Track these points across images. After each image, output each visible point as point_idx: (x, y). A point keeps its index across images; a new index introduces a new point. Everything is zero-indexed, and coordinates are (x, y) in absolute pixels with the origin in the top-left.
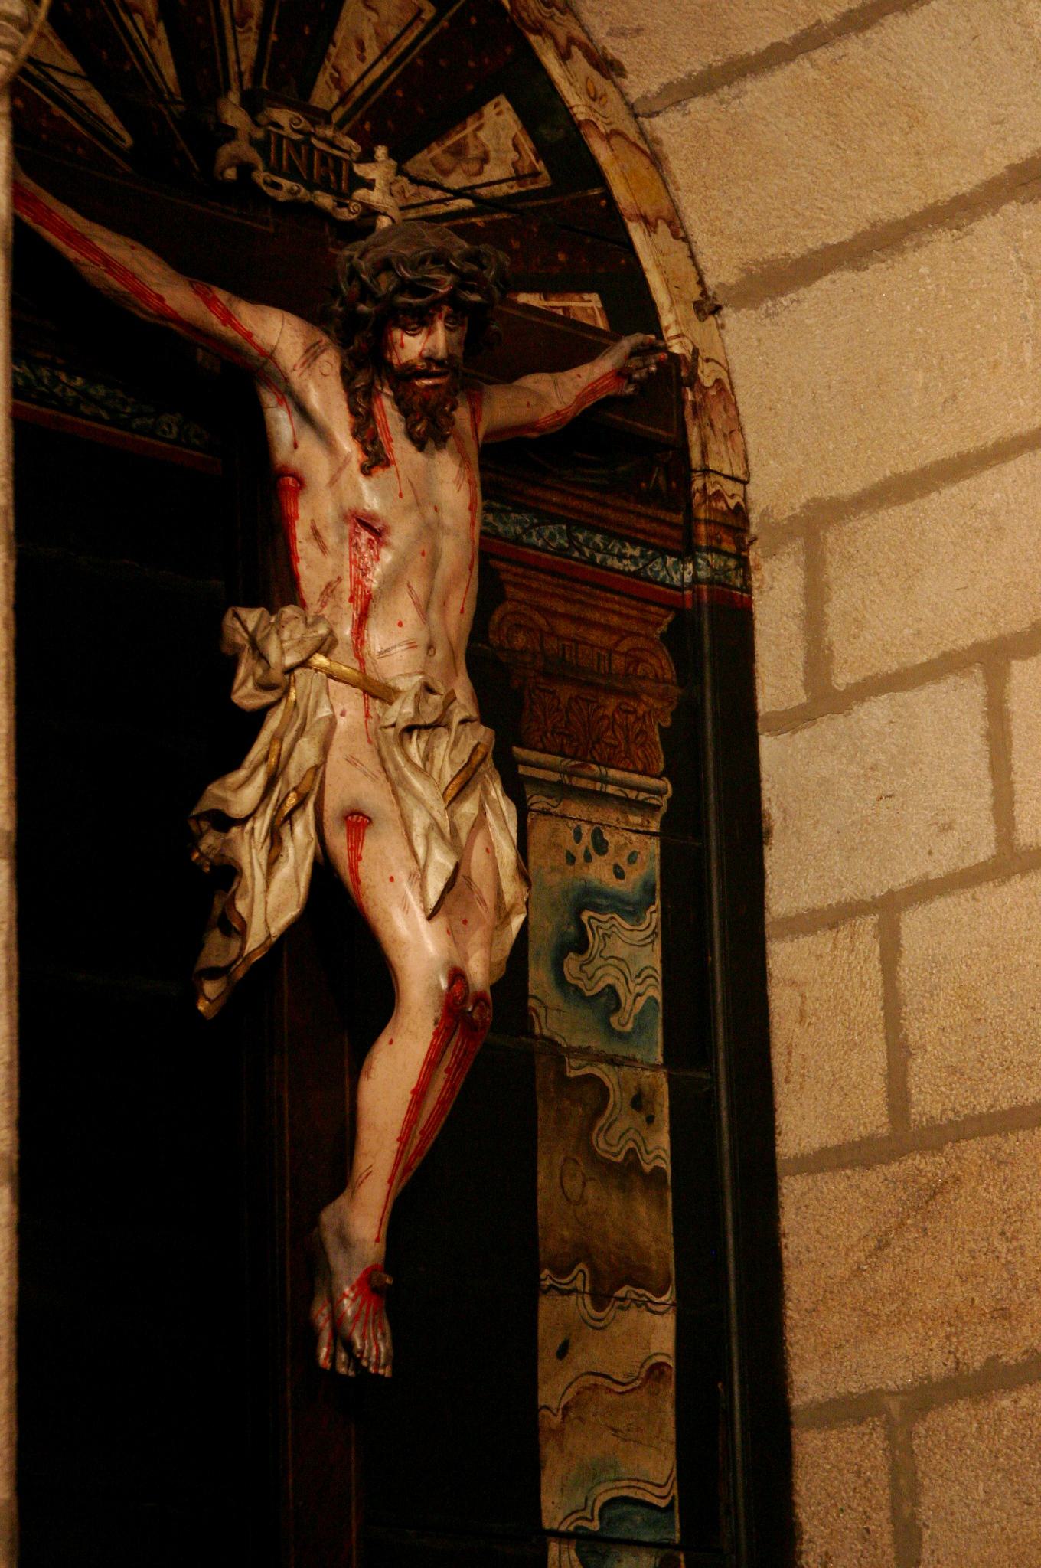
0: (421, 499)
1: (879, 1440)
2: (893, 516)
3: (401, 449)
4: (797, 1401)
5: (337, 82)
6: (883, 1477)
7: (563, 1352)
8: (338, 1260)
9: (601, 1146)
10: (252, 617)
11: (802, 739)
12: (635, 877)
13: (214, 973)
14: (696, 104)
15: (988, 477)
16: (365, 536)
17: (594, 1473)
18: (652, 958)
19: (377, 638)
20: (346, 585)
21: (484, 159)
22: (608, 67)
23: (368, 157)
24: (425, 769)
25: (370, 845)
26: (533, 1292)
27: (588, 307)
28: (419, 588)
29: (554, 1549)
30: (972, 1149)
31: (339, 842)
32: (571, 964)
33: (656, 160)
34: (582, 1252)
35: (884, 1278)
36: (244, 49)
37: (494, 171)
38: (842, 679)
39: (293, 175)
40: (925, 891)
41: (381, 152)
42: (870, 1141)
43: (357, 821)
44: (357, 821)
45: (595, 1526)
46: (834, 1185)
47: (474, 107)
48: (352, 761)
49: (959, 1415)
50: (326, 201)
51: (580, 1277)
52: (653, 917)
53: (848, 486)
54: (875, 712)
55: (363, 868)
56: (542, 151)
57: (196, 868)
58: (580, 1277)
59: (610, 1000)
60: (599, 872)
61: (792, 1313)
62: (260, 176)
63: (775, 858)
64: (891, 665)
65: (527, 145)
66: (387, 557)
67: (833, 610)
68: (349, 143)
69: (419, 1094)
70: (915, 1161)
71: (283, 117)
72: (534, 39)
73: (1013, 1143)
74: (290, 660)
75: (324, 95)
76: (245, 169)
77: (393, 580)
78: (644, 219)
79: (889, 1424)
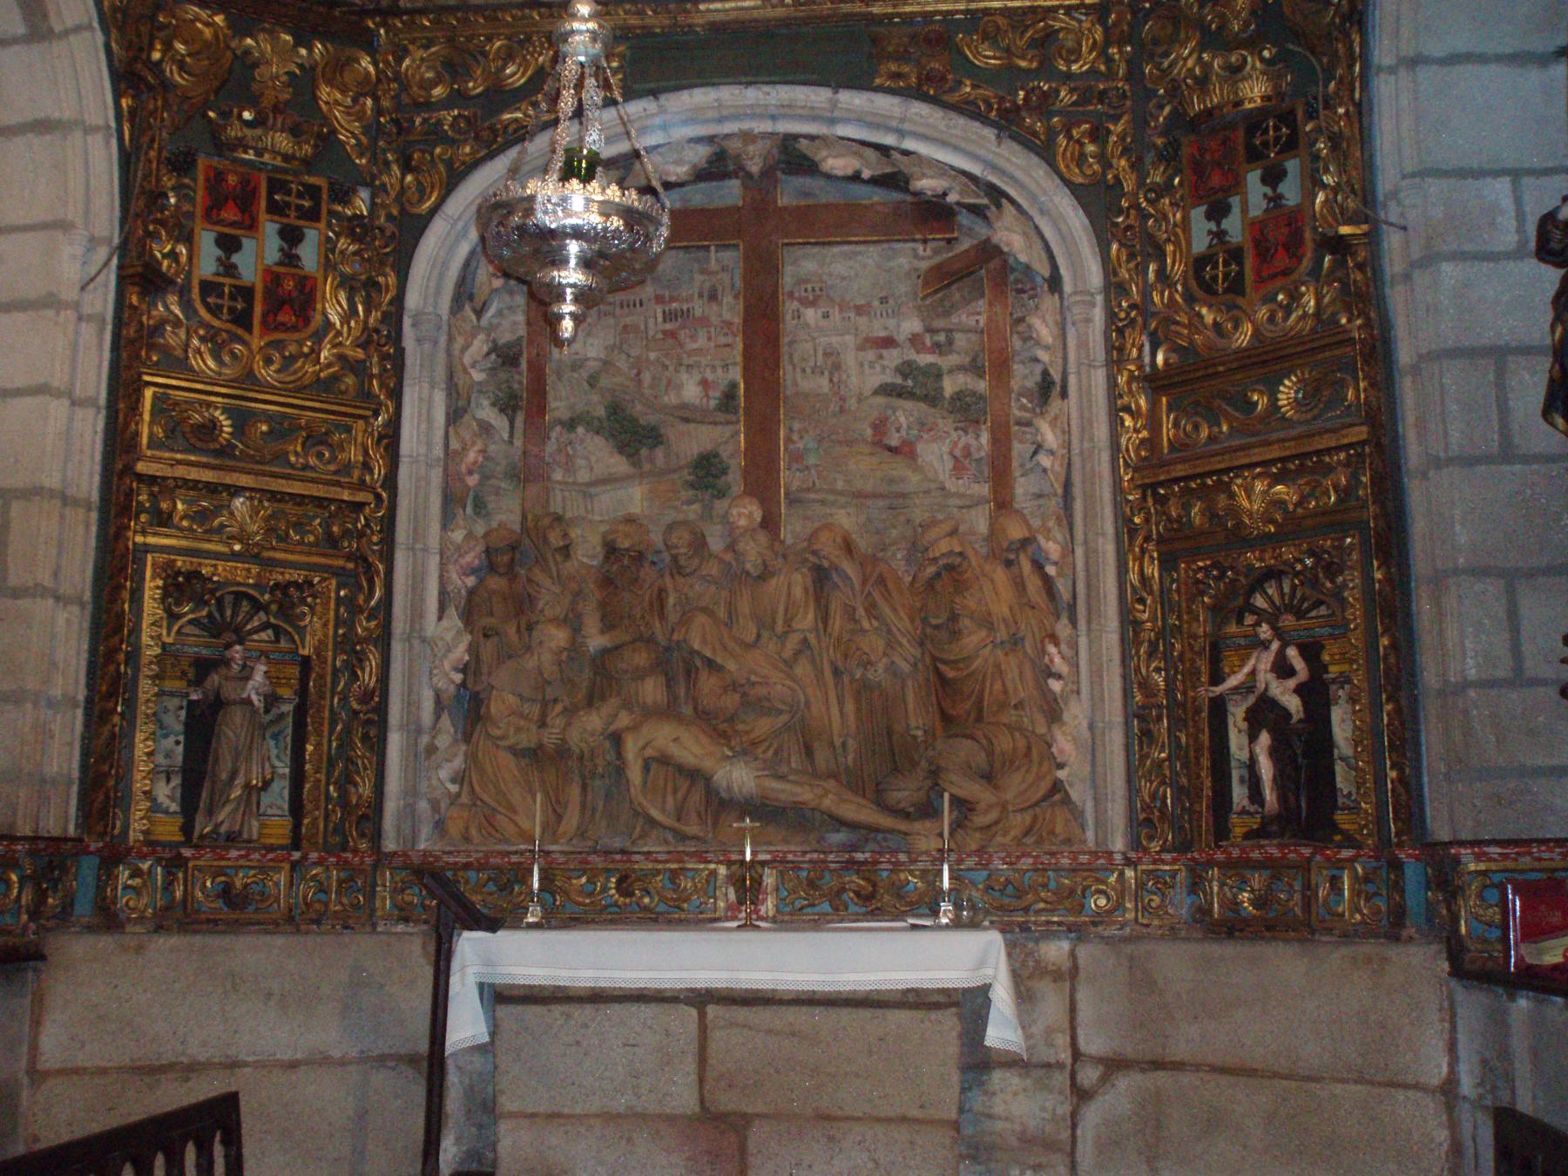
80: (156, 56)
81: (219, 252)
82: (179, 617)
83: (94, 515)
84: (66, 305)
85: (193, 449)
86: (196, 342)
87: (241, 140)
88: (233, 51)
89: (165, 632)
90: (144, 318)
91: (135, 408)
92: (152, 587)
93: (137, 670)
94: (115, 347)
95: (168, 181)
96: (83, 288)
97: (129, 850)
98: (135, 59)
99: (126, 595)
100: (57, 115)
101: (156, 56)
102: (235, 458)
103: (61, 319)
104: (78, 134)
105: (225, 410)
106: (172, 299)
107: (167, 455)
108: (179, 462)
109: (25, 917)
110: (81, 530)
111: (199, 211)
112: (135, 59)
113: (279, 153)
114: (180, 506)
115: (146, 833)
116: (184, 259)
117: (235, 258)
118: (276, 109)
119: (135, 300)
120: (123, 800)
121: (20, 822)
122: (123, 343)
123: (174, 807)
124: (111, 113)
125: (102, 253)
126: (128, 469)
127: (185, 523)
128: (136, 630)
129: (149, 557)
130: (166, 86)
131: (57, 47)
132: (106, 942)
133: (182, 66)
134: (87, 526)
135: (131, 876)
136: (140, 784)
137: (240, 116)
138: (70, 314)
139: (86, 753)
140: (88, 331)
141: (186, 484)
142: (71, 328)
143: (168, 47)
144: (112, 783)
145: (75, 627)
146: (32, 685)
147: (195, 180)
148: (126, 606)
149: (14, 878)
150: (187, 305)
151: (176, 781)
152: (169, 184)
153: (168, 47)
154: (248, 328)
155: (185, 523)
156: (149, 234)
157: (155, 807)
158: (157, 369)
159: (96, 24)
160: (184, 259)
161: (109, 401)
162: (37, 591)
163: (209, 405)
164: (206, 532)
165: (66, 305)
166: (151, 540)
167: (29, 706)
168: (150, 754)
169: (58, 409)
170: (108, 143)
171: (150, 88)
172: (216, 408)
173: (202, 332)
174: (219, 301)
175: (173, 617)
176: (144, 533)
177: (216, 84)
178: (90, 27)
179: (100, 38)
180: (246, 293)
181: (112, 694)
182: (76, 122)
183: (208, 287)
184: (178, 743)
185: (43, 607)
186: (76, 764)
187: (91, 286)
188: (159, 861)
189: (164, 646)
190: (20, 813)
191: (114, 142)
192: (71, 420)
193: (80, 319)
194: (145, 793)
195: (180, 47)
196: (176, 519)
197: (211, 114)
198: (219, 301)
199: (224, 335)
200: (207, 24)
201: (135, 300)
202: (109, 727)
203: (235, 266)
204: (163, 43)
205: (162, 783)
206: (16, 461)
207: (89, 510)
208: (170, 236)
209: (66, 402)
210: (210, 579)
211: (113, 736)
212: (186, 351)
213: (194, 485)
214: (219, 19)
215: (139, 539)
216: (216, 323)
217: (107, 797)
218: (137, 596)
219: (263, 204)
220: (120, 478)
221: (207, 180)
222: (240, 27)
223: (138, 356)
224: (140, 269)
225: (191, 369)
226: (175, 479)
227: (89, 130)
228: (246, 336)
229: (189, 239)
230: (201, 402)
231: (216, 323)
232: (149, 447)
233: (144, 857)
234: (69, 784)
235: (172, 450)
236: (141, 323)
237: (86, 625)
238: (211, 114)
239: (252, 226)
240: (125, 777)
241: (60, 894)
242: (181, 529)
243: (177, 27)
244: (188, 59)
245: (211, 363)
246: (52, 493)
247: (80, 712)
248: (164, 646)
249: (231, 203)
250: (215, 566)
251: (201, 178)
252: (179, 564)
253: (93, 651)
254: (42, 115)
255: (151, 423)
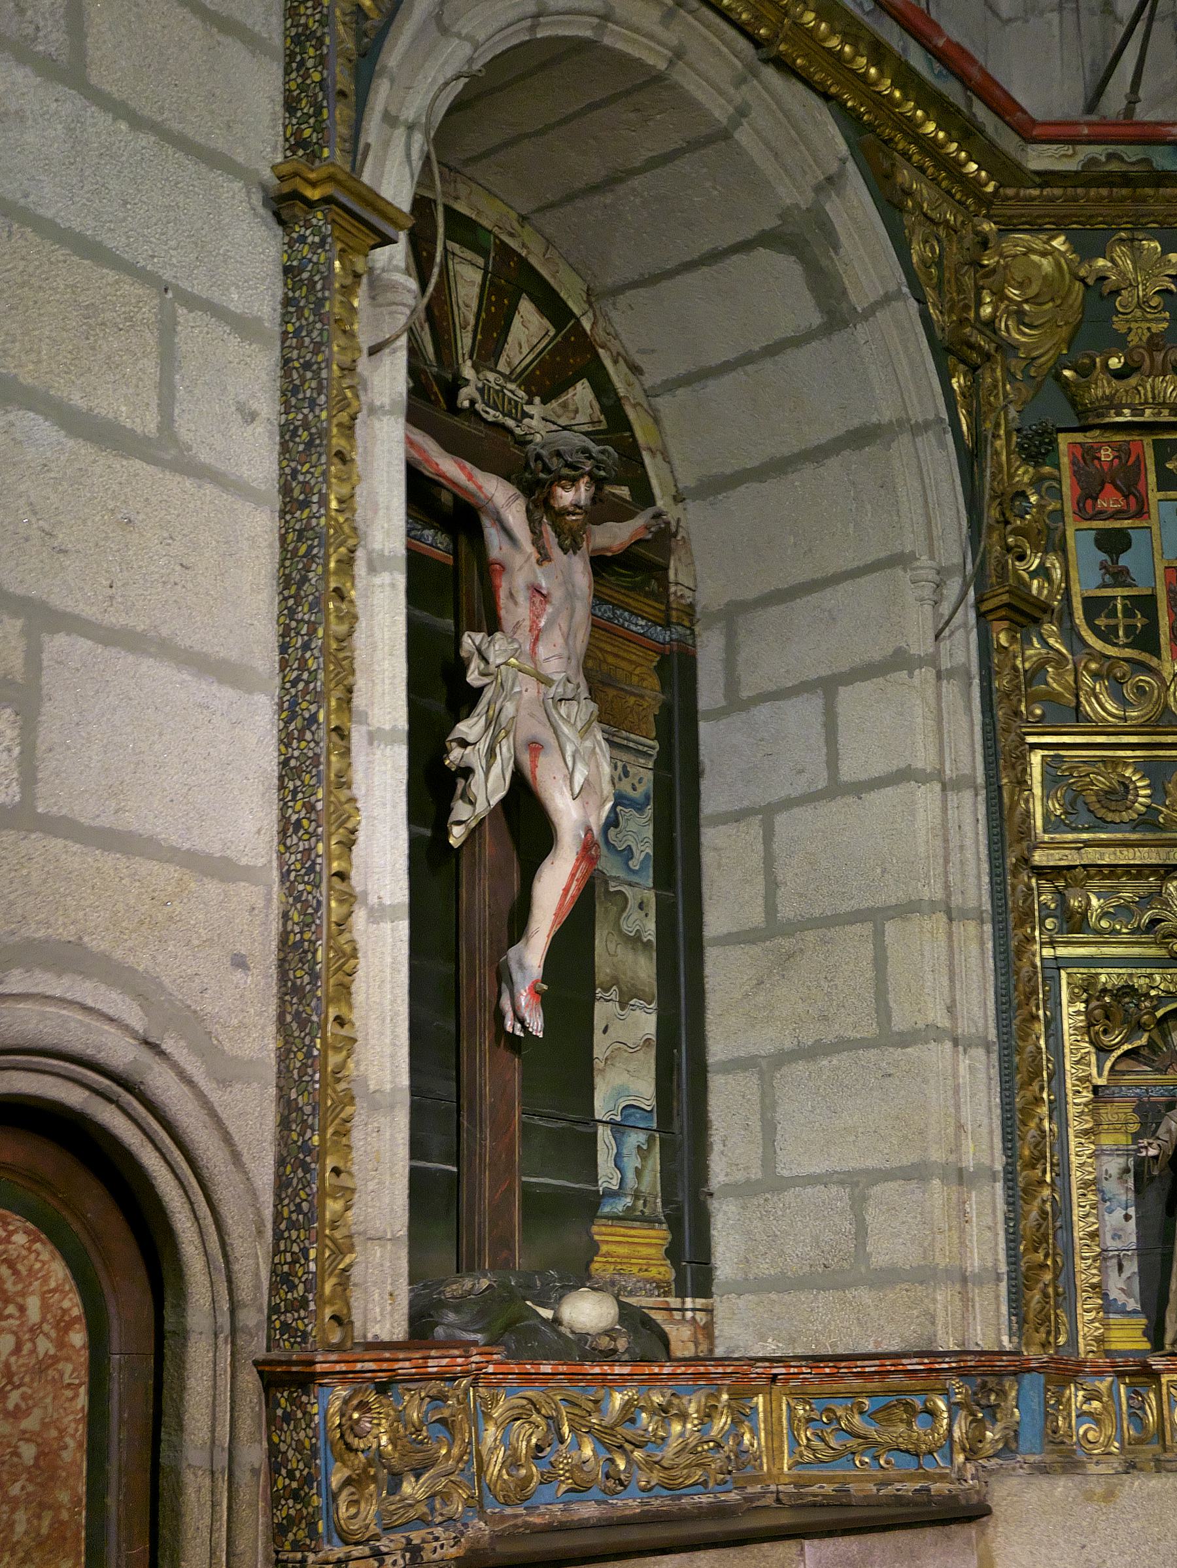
0: (568, 582)
1: (755, 1079)
2: (774, 611)
3: (556, 552)
4: (711, 1060)
5: (509, 364)
6: (756, 1098)
7: (605, 1031)
8: (517, 976)
9: (624, 927)
10: (478, 637)
11: (723, 723)
12: (641, 789)
13: (459, 823)
14: (680, 392)
15: (828, 592)
16: (538, 598)
17: (620, 1092)
18: (649, 832)
19: (542, 651)
20: (527, 623)
21: (576, 411)
22: (636, 370)
23: (530, 402)
24: (566, 721)
25: (542, 760)
26: (593, 999)
27: (624, 492)
28: (565, 628)
29: (601, 1129)
30: (810, 936)
31: (525, 759)
32: (612, 832)
33: (657, 421)
34: (615, 981)
35: (760, 999)
36: (465, 341)
37: (581, 418)
38: (745, 694)
39: (496, 408)
40: (788, 804)
41: (537, 400)
42: (755, 930)
43: (535, 747)
44: (535, 747)
45: (618, 1119)
46: (736, 952)
47: (572, 383)
48: (532, 715)
49: (800, 1068)
50: (510, 423)
51: (614, 993)
52: (649, 811)
53: (751, 594)
54: (763, 712)
55: (538, 772)
56: (604, 410)
57: (448, 769)
58: (614, 993)
59: (628, 853)
60: (625, 786)
61: (710, 1016)
62: (479, 406)
63: (705, 784)
64: (772, 687)
65: (596, 406)
66: (549, 609)
67: (742, 657)
68: (521, 393)
69: (566, 890)
70: (780, 940)
71: (491, 376)
72: (601, 351)
73: (833, 932)
74: (499, 661)
75: (502, 366)
76: (473, 402)
77: (551, 623)
78: (650, 449)
79: (761, 1074)
80: (987, 311)
81: (1104, 556)
82: (1109, 1050)
83: (988, 928)
84: (921, 662)
85: (1102, 824)
86: (1088, 680)
87: (1110, 398)
88: (1083, 280)
89: (1094, 1071)
90: (1018, 662)
91: (1022, 783)
92: (1071, 1013)
93: (1064, 1124)
94: (988, 708)
95: (1024, 474)
96: (937, 637)
97: (1081, 1363)
98: (962, 322)
99: (1040, 1028)
100: (874, 419)
101: (987, 311)
102: (1157, 827)
103: (916, 681)
104: (905, 438)
105: (1139, 766)
106: (1050, 628)
107: (1070, 837)
108: (1087, 844)
109: (960, 1458)
110: (974, 948)
111: (1069, 507)
112: (962, 322)
113: (1164, 404)
114: (1095, 902)
115: (1100, 1340)
116: (1057, 574)
117: (1124, 560)
118: (1154, 343)
119: (1003, 639)
120: (1065, 1297)
121: (940, 1333)
122: (995, 697)
123: (1133, 1304)
124: (941, 401)
125: (953, 588)
126: (1025, 861)
127: (1104, 924)
128: (1058, 1073)
129: (1063, 973)
130: (1007, 348)
131: (861, 331)
132: (1062, 1486)
133: (1020, 317)
134: (982, 943)
135: (1087, 1400)
136: (1085, 1272)
137: (1105, 365)
138: (928, 673)
139: (1013, 1239)
140: (951, 689)
141: (1099, 870)
142: (930, 692)
143: (1000, 296)
144: (1048, 1277)
145: (982, 1076)
146: (937, 1155)
147: (1057, 466)
148: (1042, 1042)
149: (942, 1405)
150: (1071, 635)
151: (1132, 1267)
152: (1026, 479)
153: (1000, 296)
154: (1156, 652)
155: (1104, 924)
156: (1009, 549)
157: (1108, 1306)
158: (1044, 725)
159: (905, 290)
160: (1057, 574)
161: (988, 776)
162: (932, 1034)
163: (1115, 762)
164: (1132, 932)
165: (921, 662)
166: (1062, 951)
167: (936, 1182)
168: (1093, 1235)
169: (927, 797)
170: (942, 445)
171: (988, 357)
172: (1127, 765)
173: (1093, 666)
174: (1112, 622)
175: (1103, 1051)
176: (1052, 944)
177: (1065, 332)
178: (898, 295)
179: (913, 305)
180: (1147, 604)
181: (1038, 1158)
182: (900, 422)
183: (1093, 606)
184: (1127, 1217)
185: (939, 1054)
186: (1002, 1256)
187: (946, 632)
188: (1120, 1375)
189: (1096, 1089)
190: (940, 1322)
191: (949, 438)
192: (945, 810)
193: (939, 676)
194: (1094, 1286)
195: (1013, 293)
196: (1093, 921)
197: (1067, 373)
198: (1112, 622)
199: (1126, 667)
200: (1044, 254)
201: (1003, 639)
202: (1037, 1202)
203: (1125, 571)
204: (993, 293)
205: (1113, 1273)
206: (884, 871)
207: (982, 922)
208: (1036, 548)
209: (937, 787)
210: (1147, 995)
211: (1043, 1213)
212: (1077, 696)
213: (1113, 870)
214: (1059, 243)
215: (1047, 952)
216: (1111, 651)
217: (1046, 1295)
218: (1053, 1026)
219: (1152, 478)
220: (1014, 876)
221: (1073, 463)
222: (1086, 248)
223: (1017, 713)
224: (1005, 598)
225: (1088, 719)
226: (1084, 866)
227: (918, 429)
228: (1154, 662)
229: (1062, 549)
230: (1104, 760)
231: (1111, 651)
232: (1045, 831)
233: (1100, 1374)
234: (998, 1279)
235: (1075, 830)
236: (1015, 668)
237: (995, 1072)
238: (1067, 373)
239: (1141, 511)
240: (1065, 1272)
241: (999, 1425)
242: (1099, 932)
243: (1006, 266)
244: (1026, 307)
245: (1111, 706)
246: (933, 906)
247: (999, 1186)
248: (1096, 1089)
249: (1109, 487)
250: (1150, 976)
251: (1065, 460)
252: (1103, 978)
253: (1007, 1107)
254: (856, 423)
255: (1046, 796)
